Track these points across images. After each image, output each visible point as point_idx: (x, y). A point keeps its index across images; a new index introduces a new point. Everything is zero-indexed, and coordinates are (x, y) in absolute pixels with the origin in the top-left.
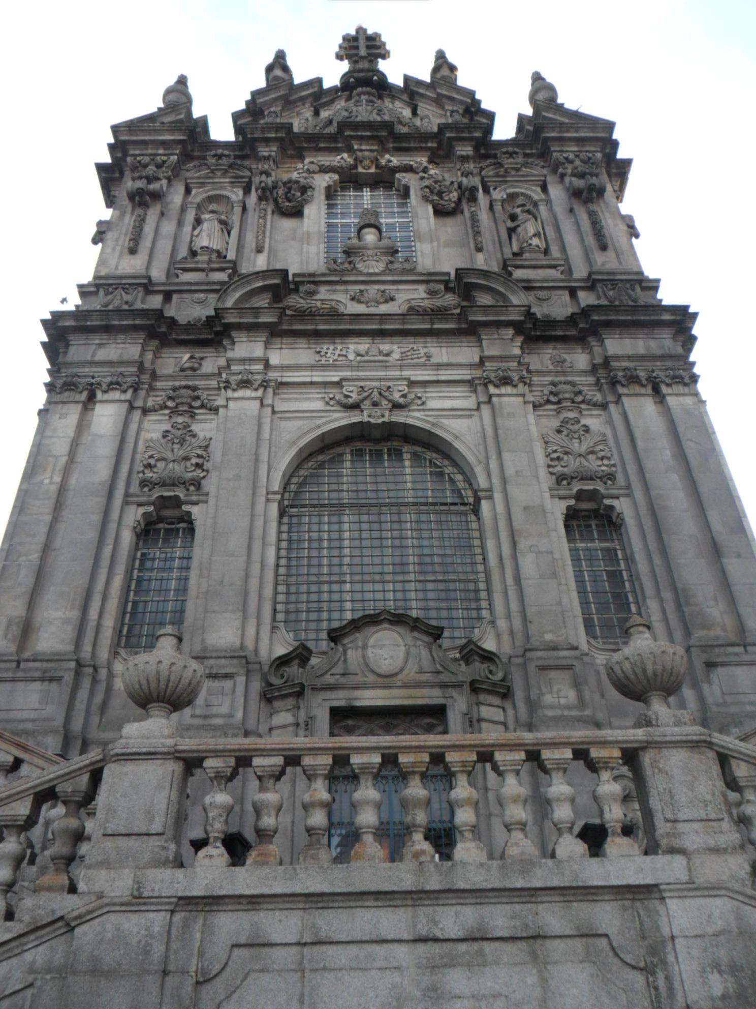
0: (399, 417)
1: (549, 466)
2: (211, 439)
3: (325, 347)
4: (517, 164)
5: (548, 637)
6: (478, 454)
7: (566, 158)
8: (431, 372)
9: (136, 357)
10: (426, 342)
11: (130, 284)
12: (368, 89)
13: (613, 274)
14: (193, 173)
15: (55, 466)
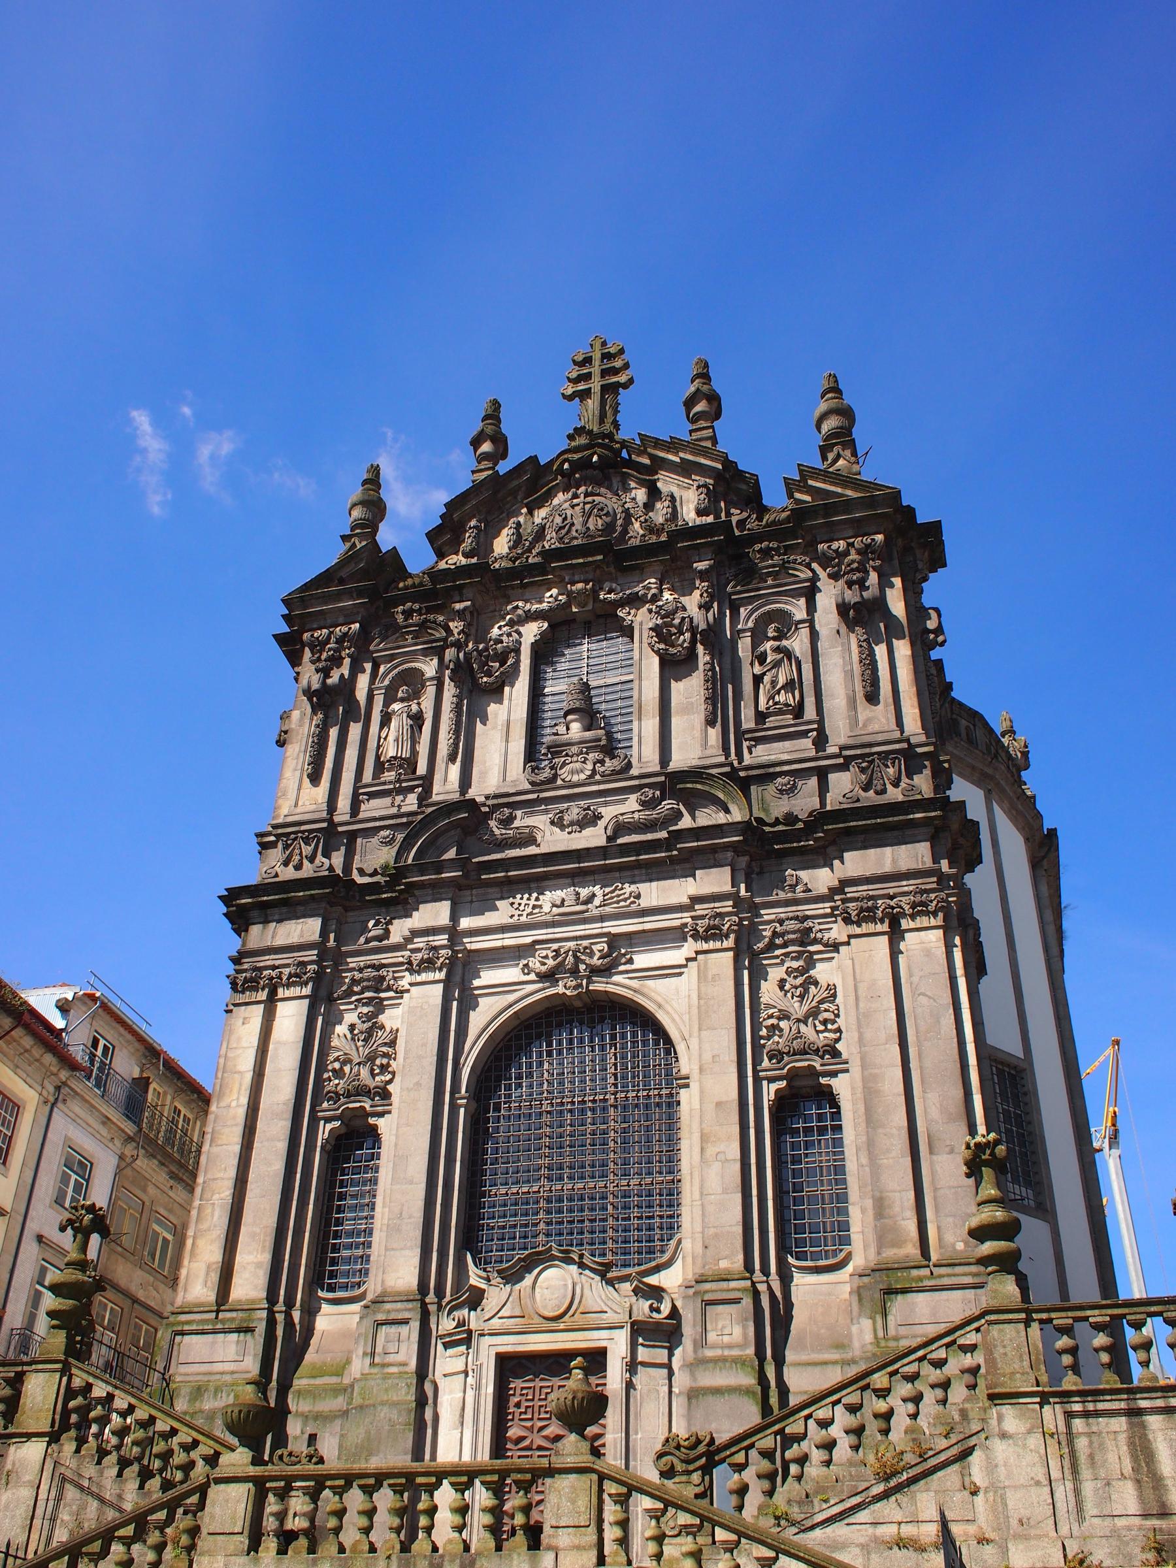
0: (599, 985)
2: (397, 1030)
3: (519, 896)
4: (773, 566)
5: (724, 1264)
6: (683, 1028)
7: (836, 551)
8: (636, 920)
9: (315, 937)
10: (634, 876)
11: (311, 831)
12: (589, 472)
13: (871, 745)
14: (377, 647)
15: (241, 1085)
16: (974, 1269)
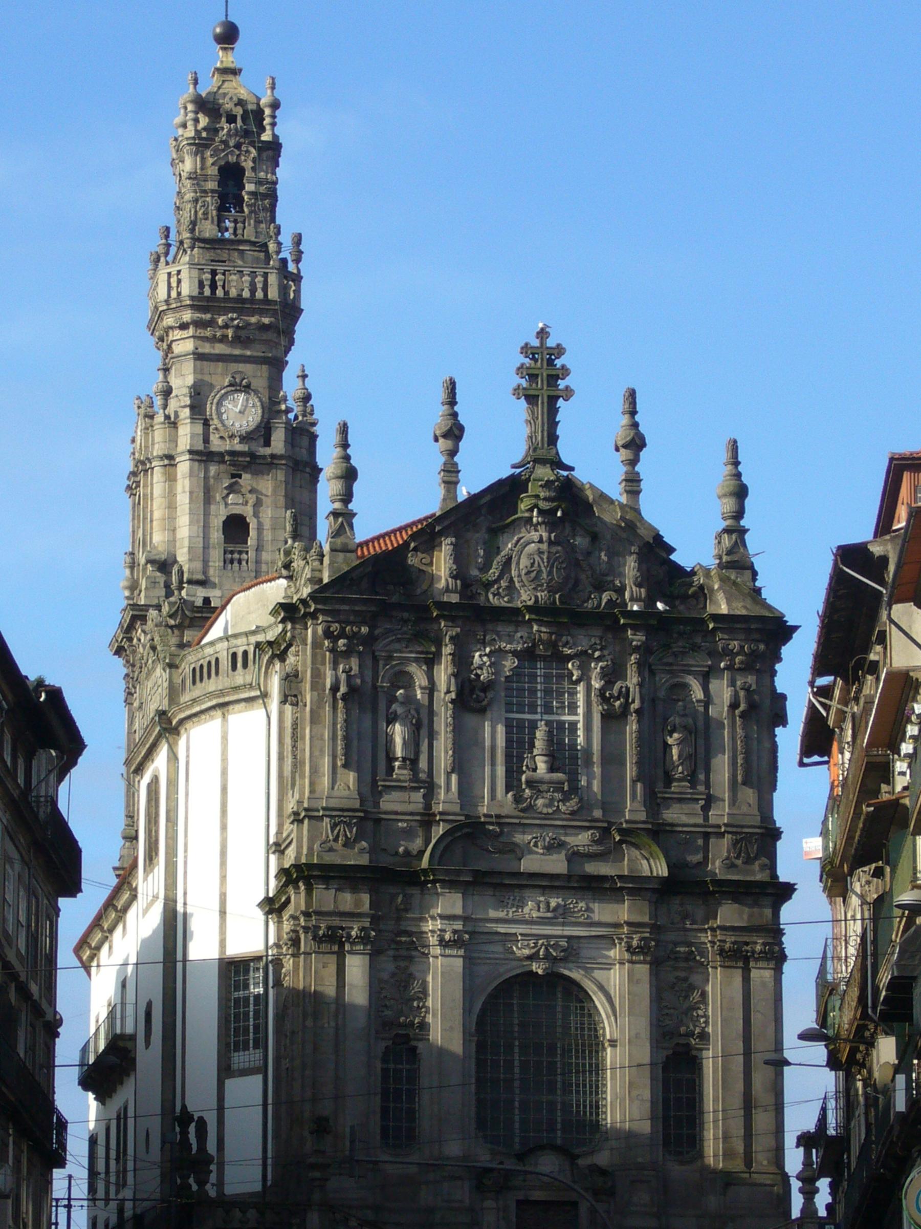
1: (659, 1021)
5: (640, 1160)
13: (742, 827)
16: (771, 1176)
